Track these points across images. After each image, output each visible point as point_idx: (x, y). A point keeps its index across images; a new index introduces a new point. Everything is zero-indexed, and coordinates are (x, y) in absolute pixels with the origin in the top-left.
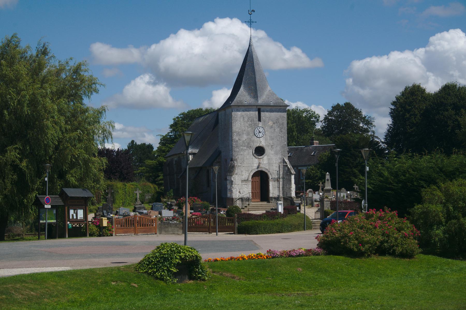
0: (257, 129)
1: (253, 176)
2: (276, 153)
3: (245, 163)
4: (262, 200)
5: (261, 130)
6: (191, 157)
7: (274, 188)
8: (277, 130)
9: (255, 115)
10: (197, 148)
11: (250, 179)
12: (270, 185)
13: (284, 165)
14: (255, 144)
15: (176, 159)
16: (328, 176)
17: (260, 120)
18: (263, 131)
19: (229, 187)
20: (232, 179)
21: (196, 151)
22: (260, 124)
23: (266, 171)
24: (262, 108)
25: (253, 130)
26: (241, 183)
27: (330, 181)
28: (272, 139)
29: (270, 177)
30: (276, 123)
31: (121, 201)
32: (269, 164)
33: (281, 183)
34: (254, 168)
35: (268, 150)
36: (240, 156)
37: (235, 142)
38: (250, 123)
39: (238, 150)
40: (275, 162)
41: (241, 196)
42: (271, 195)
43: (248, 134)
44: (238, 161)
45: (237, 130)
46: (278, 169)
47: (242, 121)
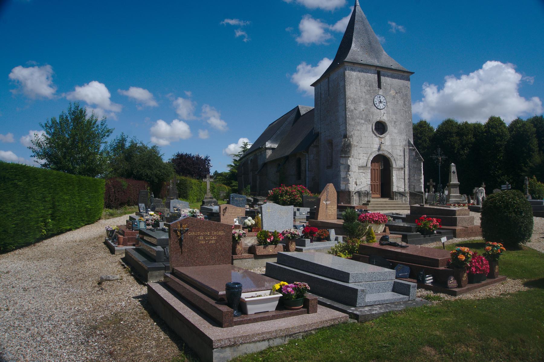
0: (376, 97)
1: (373, 162)
2: (400, 133)
3: (363, 142)
4: (383, 196)
5: (382, 99)
6: (269, 153)
7: (398, 179)
8: (401, 102)
10: (277, 143)
11: (369, 165)
12: (394, 175)
13: (410, 149)
14: (375, 118)
15: (251, 158)
16: (453, 168)
17: (379, 86)
18: (385, 101)
19: (343, 174)
20: (349, 163)
21: (275, 146)
22: (381, 92)
23: (389, 156)
24: (382, 71)
25: (372, 98)
26: (357, 171)
27: (456, 173)
28: (395, 113)
29: (394, 166)
30: (399, 93)
31: (195, 198)
32: (392, 145)
33: (407, 172)
34: (374, 150)
35: (390, 128)
36: (356, 132)
38: (369, 88)
39: (353, 123)
40: (399, 144)
41: (358, 188)
42: (395, 189)
43: (366, 103)
44: (354, 138)
45: (352, 96)
46: (402, 154)
47: (358, 84)
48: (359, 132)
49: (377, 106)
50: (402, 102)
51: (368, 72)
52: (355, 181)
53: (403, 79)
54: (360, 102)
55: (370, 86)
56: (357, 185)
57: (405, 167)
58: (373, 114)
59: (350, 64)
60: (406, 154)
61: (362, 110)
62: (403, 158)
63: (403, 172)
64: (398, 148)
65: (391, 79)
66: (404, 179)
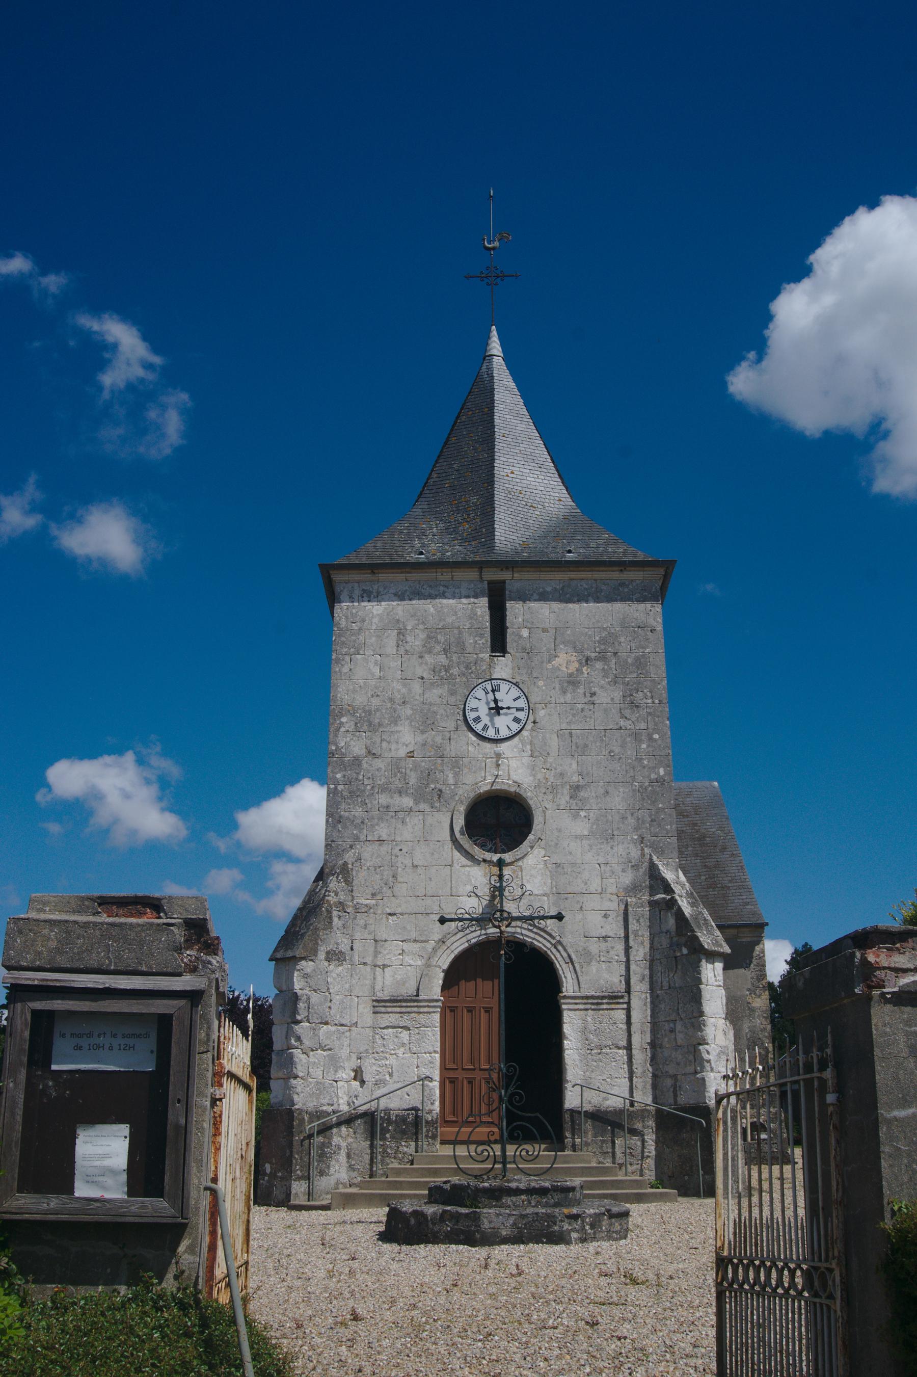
0: (479, 693)
3: (401, 889)
5: (507, 696)
7: (594, 1050)
8: (609, 696)
9: (472, 616)
12: (567, 1029)
17: (499, 644)
18: (522, 703)
22: (503, 667)
24: (514, 580)
25: (460, 698)
28: (579, 750)
29: (569, 986)
30: (602, 657)
35: (548, 816)
36: (369, 853)
37: (343, 766)
38: (443, 659)
40: (595, 885)
44: (359, 876)
45: (360, 700)
46: (615, 928)
48: (385, 848)
49: (478, 727)
50: (618, 694)
51: (443, 596)
52: (354, 1063)
53: (623, 599)
54: (395, 720)
55: (446, 651)
56: (363, 1082)
57: (628, 991)
58: (457, 765)
59: (355, 576)
60: (633, 926)
61: (402, 752)
62: (620, 947)
63: (621, 1015)
64: (593, 902)
65: (556, 606)
66: (629, 1048)
